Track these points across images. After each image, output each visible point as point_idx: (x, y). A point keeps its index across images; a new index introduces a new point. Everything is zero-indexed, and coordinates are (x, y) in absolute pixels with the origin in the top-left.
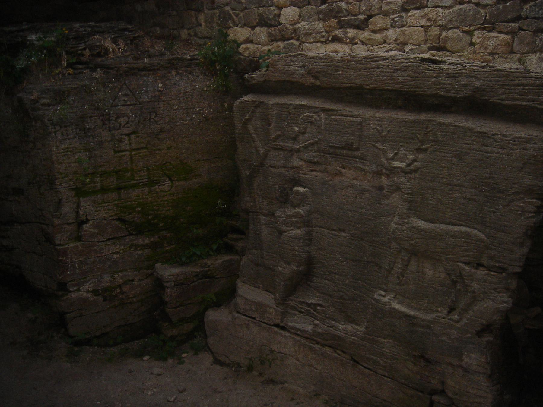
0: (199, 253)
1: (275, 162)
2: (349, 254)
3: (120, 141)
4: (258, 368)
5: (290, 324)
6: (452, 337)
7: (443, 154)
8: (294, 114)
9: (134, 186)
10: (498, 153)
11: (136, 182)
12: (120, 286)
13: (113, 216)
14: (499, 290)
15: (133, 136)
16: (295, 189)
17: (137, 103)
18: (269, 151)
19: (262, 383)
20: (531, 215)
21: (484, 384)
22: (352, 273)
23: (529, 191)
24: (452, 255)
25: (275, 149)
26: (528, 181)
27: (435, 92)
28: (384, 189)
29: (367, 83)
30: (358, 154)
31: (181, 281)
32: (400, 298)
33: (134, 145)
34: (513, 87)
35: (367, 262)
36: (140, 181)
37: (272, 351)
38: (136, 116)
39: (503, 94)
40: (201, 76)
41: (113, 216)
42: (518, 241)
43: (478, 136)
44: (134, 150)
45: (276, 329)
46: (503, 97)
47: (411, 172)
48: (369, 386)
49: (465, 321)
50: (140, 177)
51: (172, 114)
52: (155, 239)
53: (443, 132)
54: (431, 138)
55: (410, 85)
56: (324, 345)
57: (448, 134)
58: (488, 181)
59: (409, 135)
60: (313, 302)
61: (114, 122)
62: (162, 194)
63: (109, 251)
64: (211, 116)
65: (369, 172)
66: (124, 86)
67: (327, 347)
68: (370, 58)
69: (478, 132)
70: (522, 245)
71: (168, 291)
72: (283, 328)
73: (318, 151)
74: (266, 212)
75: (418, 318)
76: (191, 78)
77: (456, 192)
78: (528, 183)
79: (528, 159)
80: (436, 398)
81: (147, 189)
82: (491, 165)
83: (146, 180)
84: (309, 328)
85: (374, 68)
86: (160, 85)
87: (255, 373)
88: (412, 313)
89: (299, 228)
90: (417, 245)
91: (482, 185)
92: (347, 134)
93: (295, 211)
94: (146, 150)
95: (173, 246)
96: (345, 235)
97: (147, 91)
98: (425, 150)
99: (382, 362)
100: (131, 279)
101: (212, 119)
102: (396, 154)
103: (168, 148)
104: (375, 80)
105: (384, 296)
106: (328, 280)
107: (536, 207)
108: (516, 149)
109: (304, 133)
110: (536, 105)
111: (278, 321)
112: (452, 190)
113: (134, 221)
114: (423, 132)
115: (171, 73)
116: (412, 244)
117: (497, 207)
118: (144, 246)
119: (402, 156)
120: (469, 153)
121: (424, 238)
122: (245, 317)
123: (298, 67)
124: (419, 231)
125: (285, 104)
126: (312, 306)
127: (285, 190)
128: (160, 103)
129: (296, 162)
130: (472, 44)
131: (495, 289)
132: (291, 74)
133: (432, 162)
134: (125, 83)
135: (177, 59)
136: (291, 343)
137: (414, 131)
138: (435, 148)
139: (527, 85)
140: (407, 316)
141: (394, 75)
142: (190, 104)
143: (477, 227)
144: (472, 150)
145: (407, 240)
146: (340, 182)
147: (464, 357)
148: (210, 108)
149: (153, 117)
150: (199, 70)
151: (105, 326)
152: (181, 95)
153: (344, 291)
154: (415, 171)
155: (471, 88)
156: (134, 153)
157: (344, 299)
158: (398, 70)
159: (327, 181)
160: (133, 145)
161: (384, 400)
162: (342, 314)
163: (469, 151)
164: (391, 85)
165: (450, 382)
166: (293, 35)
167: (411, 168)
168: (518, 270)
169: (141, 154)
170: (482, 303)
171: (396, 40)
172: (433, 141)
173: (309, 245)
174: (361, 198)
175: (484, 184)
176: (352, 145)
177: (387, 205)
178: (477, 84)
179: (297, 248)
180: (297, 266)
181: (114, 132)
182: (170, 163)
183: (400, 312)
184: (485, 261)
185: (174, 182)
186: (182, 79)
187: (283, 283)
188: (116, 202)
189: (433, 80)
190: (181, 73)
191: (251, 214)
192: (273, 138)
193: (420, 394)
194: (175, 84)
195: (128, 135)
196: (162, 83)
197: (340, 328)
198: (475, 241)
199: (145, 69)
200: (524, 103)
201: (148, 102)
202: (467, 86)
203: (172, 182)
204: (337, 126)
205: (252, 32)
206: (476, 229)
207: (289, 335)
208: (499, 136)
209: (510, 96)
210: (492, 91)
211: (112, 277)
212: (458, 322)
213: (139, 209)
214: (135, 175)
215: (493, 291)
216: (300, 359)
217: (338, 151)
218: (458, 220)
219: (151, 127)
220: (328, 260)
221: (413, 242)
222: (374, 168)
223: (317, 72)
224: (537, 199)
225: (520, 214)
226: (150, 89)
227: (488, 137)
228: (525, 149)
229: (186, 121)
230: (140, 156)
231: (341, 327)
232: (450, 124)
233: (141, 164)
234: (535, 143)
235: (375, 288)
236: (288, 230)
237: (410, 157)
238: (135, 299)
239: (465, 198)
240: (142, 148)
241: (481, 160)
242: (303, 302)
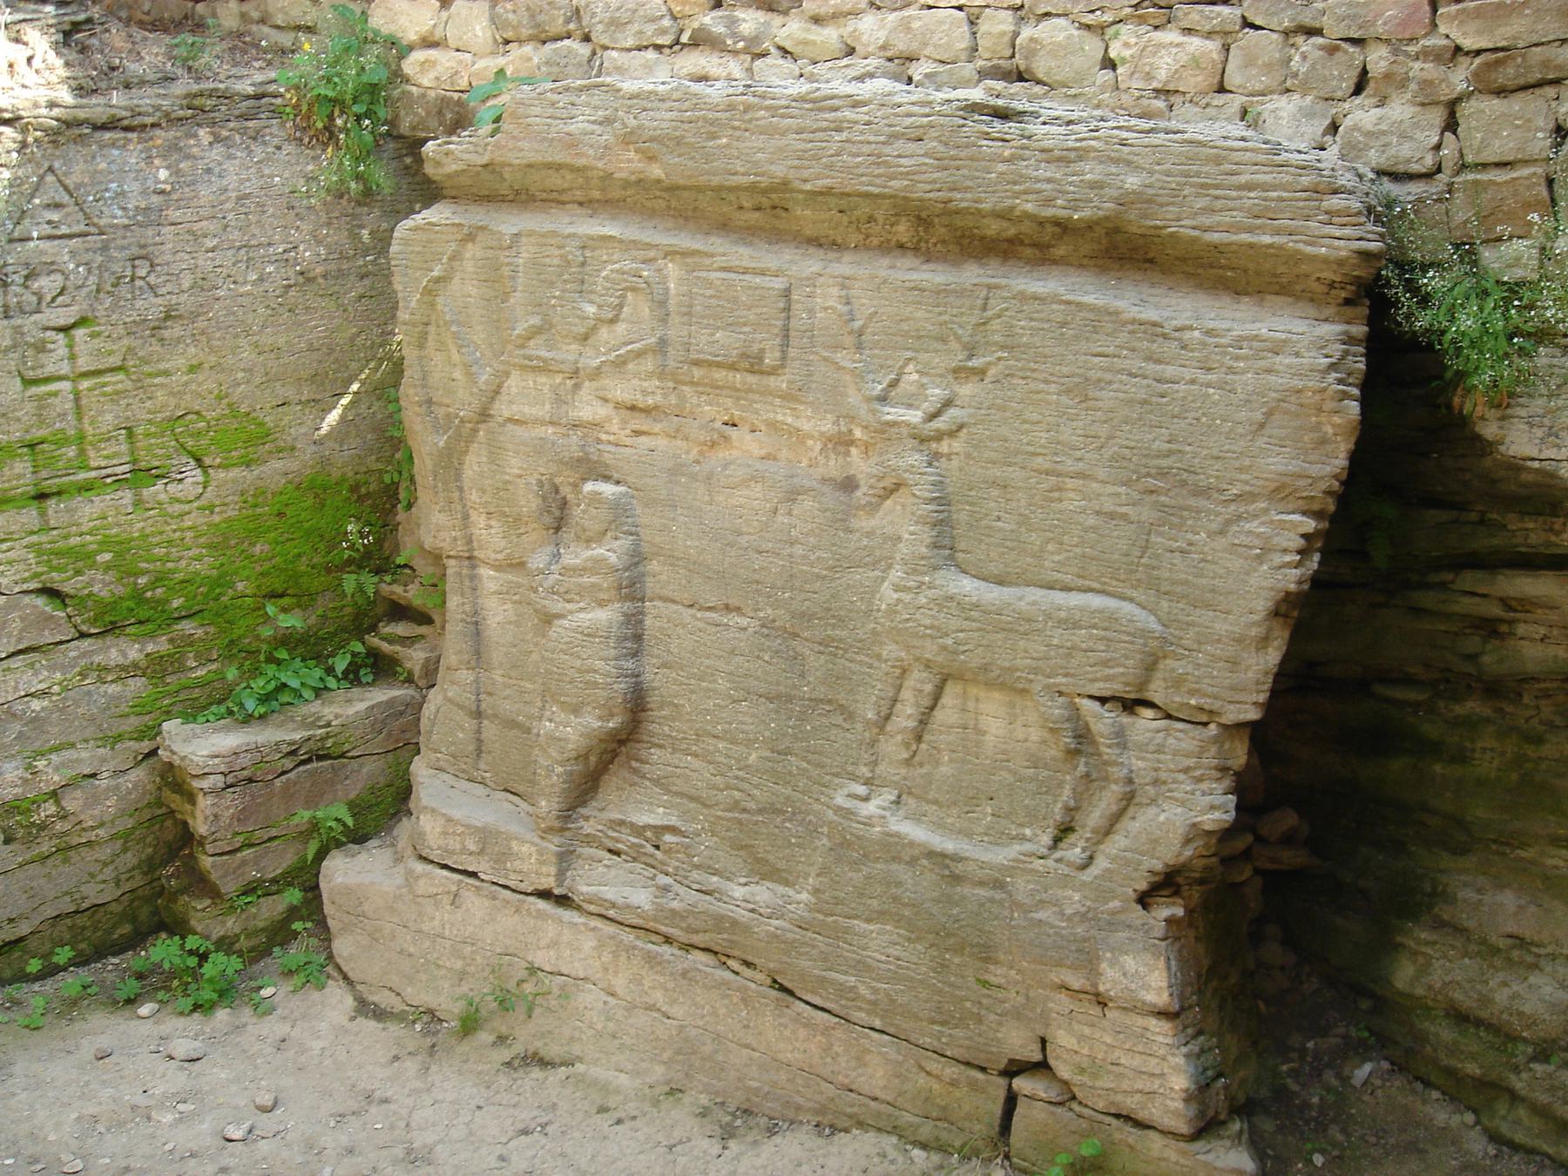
0: (294, 683)
1: (526, 409)
2: (757, 679)
3: (41, 348)
4: (489, 1022)
5: (584, 889)
6: (1069, 911)
7: (1033, 386)
8: (583, 264)
9: (86, 488)
10: (1193, 382)
11: (93, 474)
12: (54, 795)
13: (24, 581)
14: (1198, 773)
15: (79, 333)
16: (589, 487)
17: (93, 230)
18: (507, 374)
19: (508, 1064)
20: (1288, 558)
21: (1160, 1039)
22: (767, 734)
23: (1280, 493)
24: (1066, 675)
25: (523, 368)
26: (1277, 462)
27: (1009, 202)
28: (857, 487)
29: (806, 174)
31: (245, 773)
32: (911, 801)
33: (84, 363)
34: (1234, 194)
35: (811, 700)
36: (109, 471)
37: (533, 970)
38: (89, 271)
40: (288, 148)
41: (24, 581)
42: (1254, 632)
43: (1132, 332)
44: (86, 375)
45: (542, 904)
46: (1206, 220)
47: (939, 436)
48: (829, 1060)
49: (1101, 863)
50: (107, 457)
51: (200, 262)
52: (160, 646)
53: (1031, 319)
54: (997, 338)
55: (934, 181)
56: (689, 947)
58: (1164, 463)
60: (651, 822)
61: (18, 290)
62: (178, 508)
63: (16, 689)
64: (319, 270)
65: (812, 437)
66: (50, 178)
67: (697, 952)
68: (814, 101)
69: (1133, 321)
70: (1263, 642)
71: (204, 803)
72: (563, 901)
73: (662, 374)
74: (500, 557)
75: (967, 859)
76: (259, 152)
77: (1072, 495)
78: (1281, 468)
80: (1021, 1084)
81: (127, 496)
82: (1174, 417)
83: (126, 468)
84: (642, 898)
85: (825, 130)
86: (163, 174)
87: (485, 1037)
88: (950, 846)
89: (602, 604)
90: (962, 648)
91: (1148, 475)
92: (745, 325)
93: (590, 553)
94: (121, 376)
95: (214, 667)
96: (744, 622)
97: (123, 194)
98: (981, 373)
99: (863, 991)
100: (87, 771)
101: (325, 276)
102: (894, 384)
103: (192, 369)
104: (830, 167)
105: (866, 799)
106: (696, 756)
107: (1303, 536)
108: (1244, 372)
109: (613, 321)
110: (1301, 246)
111: (548, 882)
112: (1060, 489)
113: (89, 595)
114: (974, 320)
115: (195, 136)
116: (944, 648)
117: (1189, 536)
118: (127, 671)
119: (913, 389)
120: (1110, 382)
121: (979, 630)
122: (445, 873)
123: (594, 122)
124: (968, 608)
125: (554, 234)
126: (649, 834)
127: (557, 492)
128: (165, 230)
129: (587, 408)
130: (1109, 64)
131: (1186, 770)
132: (571, 142)
133: (1003, 409)
134: (51, 169)
135: (210, 94)
136: (588, 944)
137: (946, 318)
138: (1007, 368)
139: (1274, 188)
140: (931, 854)
141: (887, 150)
142: (257, 231)
143: (1129, 593)
144: (1121, 371)
145: (930, 636)
146: (725, 467)
147: (1104, 965)
148: (319, 243)
149: (142, 272)
150: (283, 125)
151: (11, 920)
152: (228, 206)
153: (746, 786)
154: (952, 434)
155: (1115, 193)
156: (85, 384)
157: (744, 810)
158: (895, 136)
159: (683, 465)
160: (81, 361)
161: (875, 1099)
162: (742, 853)
163: (1108, 376)
164: (878, 181)
165: (1063, 1039)
166: (572, 26)
167: (940, 424)
168: (1253, 715)
169: (108, 389)
170: (1152, 811)
171: (883, 48)
172: (1003, 348)
173: (635, 654)
174: (790, 514)
175: (1153, 471)
176: (760, 357)
177: (870, 534)
178: (1132, 181)
179: (599, 664)
180: (600, 718)
181: (19, 322)
182: (197, 413)
183: (912, 844)
184: (1156, 693)
185: (211, 471)
186: (230, 157)
187: (560, 769)
188: (34, 538)
189: (1001, 167)
190: (227, 138)
191: (452, 562)
192: (518, 336)
193: (980, 1076)
194: (209, 171)
195: (64, 329)
196: (168, 168)
197: (737, 895)
198: (1129, 634)
199: (110, 125)
200: (1267, 239)
201: (126, 227)
202: (1102, 188)
203: (205, 472)
204: (713, 302)
205: (444, 14)
206: (1131, 600)
207: (582, 920)
208: (1196, 333)
209: (1226, 218)
210: (1172, 204)
211: (29, 767)
212: (1084, 867)
213: (108, 556)
214: (92, 454)
215: (1181, 777)
216: (619, 991)
217: (719, 375)
218: (1079, 576)
219: (139, 304)
220: (694, 697)
221: (949, 642)
222: (827, 426)
223: (652, 139)
224: (1304, 513)
225: (1258, 556)
226: (132, 187)
227: (1165, 336)
228: (1269, 371)
229: (245, 283)
230: (104, 395)
231: (738, 892)
232: (1055, 299)
233: (109, 417)
234: (1297, 354)
235: (836, 775)
236: (571, 612)
237: (936, 393)
238: (101, 832)
239: (1097, 513)
240: (112, 370)
241: (1145, 402)
242: (622, 823)
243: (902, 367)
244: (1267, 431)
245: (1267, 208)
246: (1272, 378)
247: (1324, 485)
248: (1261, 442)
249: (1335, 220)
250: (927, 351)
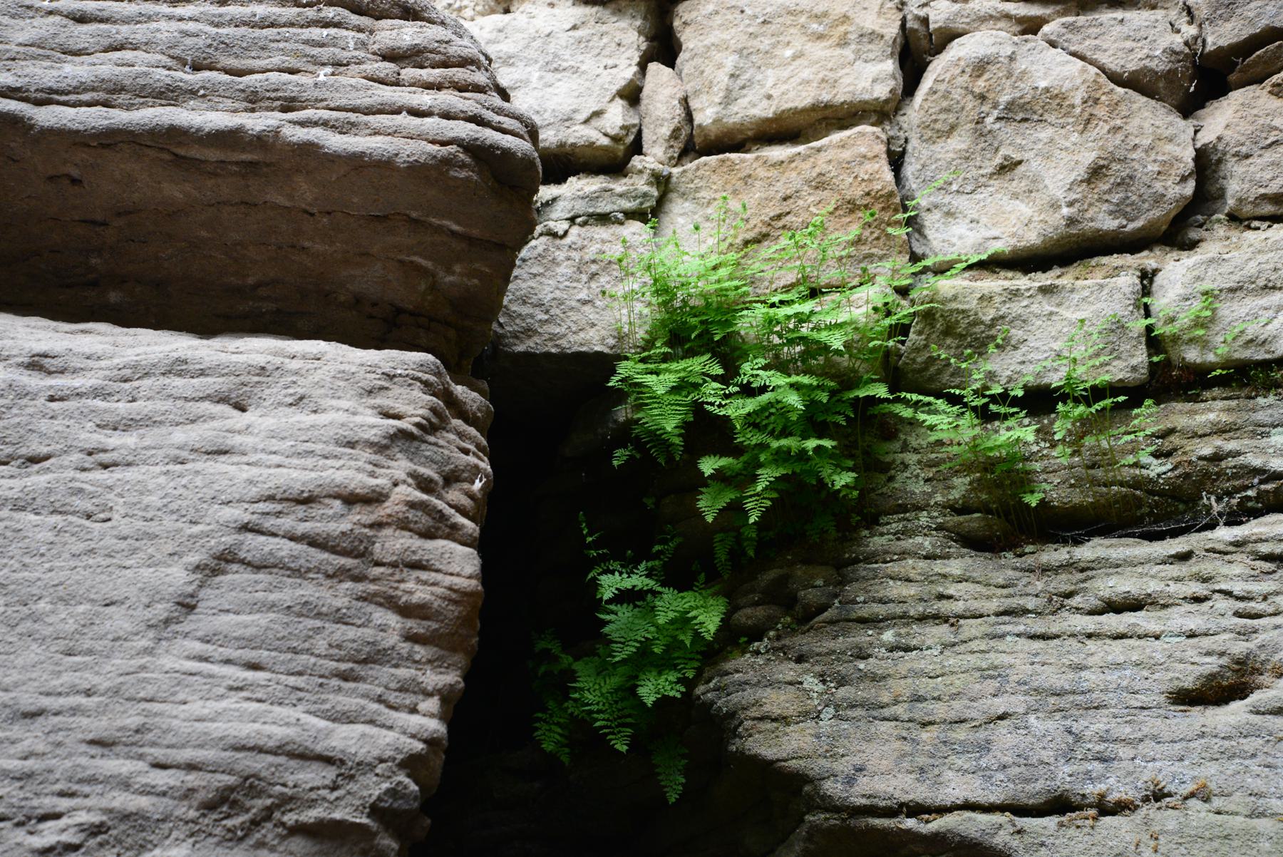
39: (40, 49)
46: (43, 74)
78: (245, 730)
79: (246, 528)
209: (105, 67)
244: (202, 622)
245: (226, 46)
246: (221, 466)
247: (373, 788)
248: (172, 659)
249: (409, 73)
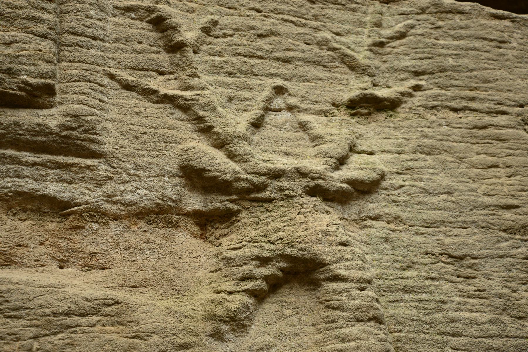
7: (471, 118)
30: (51, 118)
53: (455, 38)
54: (407, 62)
57: (477, 44)
59: (304, 46)
98: (388, 106)
137: (328, 36)
138: (436, 97)
172: (417, 74)
243: (269, 100)
250: (303, 79)
